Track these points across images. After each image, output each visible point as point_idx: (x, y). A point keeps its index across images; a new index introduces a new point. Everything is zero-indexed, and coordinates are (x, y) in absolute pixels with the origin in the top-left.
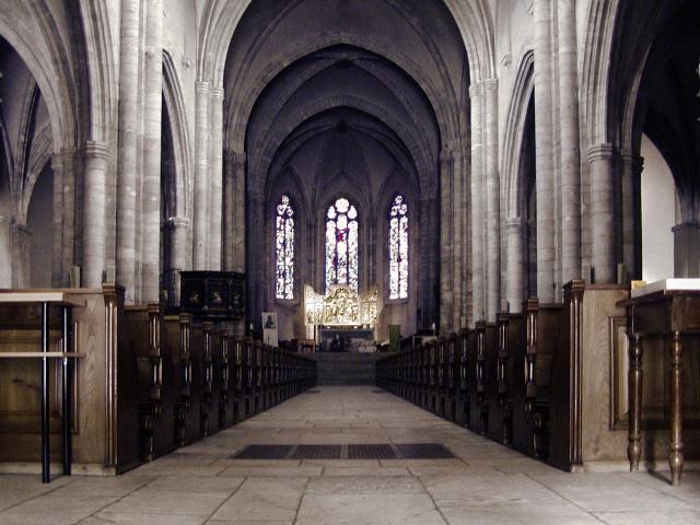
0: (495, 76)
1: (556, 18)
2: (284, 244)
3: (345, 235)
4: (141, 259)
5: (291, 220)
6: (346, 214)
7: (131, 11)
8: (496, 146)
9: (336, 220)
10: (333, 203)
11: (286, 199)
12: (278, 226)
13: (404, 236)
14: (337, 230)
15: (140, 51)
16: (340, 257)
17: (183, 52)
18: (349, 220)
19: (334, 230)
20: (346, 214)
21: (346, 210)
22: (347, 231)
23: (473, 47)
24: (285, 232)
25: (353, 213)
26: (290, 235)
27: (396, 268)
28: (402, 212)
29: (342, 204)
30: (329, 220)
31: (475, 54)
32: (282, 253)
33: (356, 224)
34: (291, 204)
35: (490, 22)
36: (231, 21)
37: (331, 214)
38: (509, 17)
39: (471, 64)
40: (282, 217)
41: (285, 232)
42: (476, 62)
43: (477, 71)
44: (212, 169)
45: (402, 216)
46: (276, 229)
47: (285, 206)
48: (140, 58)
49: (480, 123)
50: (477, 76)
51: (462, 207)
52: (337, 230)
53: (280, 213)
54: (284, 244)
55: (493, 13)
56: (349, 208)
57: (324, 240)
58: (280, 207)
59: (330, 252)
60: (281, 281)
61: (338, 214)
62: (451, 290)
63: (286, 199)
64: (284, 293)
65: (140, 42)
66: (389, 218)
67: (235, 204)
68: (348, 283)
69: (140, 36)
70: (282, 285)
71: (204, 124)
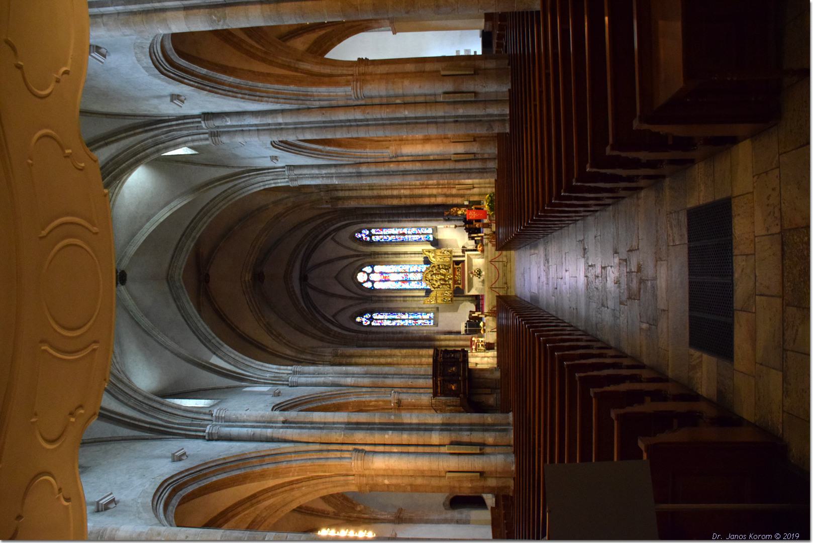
0: (284, 167)
1: (256, 125)
2: (393, 320)
3: (384, 275)
4: (438, 427)
5: (374, 314)
6: (368, 274)
7: (254, 434)
8: (335, 166)
9: (373, 282)
10: (361, 284)
11: (358, 319)
12: (379, 324)
13: (385, 232)
14: (380, 281)
15: (282, 428)
17: (268, 396)
18: (373, 272)
20: (368, 274)
21: (366, 275)
22: (381, 273)
23: (261, 184)
24: (383, 320)
25: (368, 269)
26: (385, 316)
27: (410, 236)
28: (367, 232)
29: (361, 277)
30: (373, 286)
31: (266, 183)
32: (398, 321)
34: (362, 315)
35: (243, 172)
36: (243, 361)
37: (368, 285)
38: (245, 158)
39: (273, 185)
40: (371, 321)
41: (383, 320)
42: (272, 182)
43: (279, 181)
44: (354, 374)
45: (370, 233)
46: (381, 326)
47: (364, 320)
48: (287, 428)
49: (318, 178)
50: (283, 180)
51: (373, 189)
52: (380, 281)
53: (369, 323)
54: (393, 320)
55: (237, 170)
56: (365, 272)
57: (389, 290)
58: (364, 323)
59: (398, 286)
60: (419, 322)
61: (368, 280)
62: (435, 196)
63: (358, 319)
64: (429, 320)
65: (275, 427)
66: (371, 243)
67: (371, 356)
69: (271, 427)
71: (321, 380)
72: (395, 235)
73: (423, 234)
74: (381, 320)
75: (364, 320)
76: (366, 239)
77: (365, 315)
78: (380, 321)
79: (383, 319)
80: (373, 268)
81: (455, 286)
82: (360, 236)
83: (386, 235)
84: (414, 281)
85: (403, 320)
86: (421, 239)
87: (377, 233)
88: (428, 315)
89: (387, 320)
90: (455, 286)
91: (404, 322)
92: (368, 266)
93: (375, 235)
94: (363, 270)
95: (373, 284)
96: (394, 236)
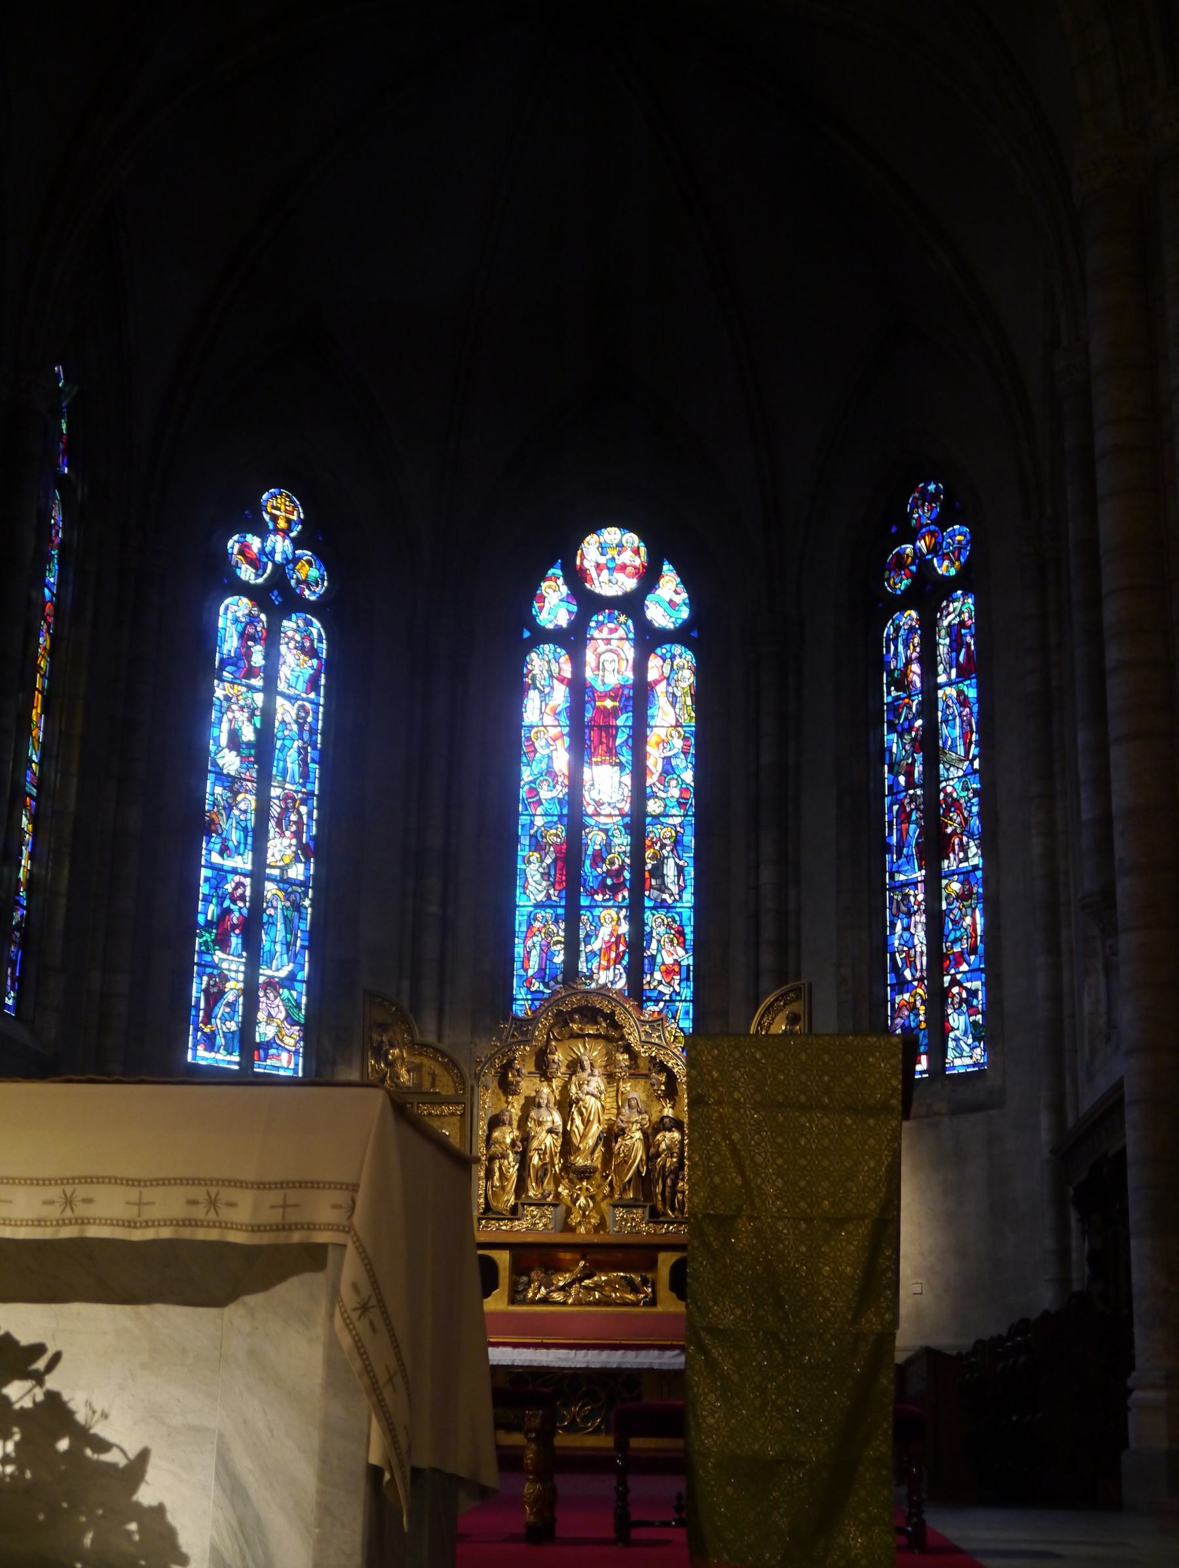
3: (624, 720)
5: (316, 628)
6: (631, 605)
12: (230, 644)
14: (578, 688)
16: (594, 840)
19: (560, 695)
20: (631, 605)
21: (630, 584)
28: (945, 569)
30: (543, 636)
32: (248, 801)
33: (685, 658)
45: (946, 588)
56: (649, 579)
58: (255, 542)
68: (637, 992)
70: (234, 988)
72: (932, 779)
73: (938, 999)
74: (271, 674)
75: (281, 546)
76: (900, 563)
77: (323, 556)
78: (258, 659)
79: (270, 688)
80: (678, 636)
81: (503, 1258)
82: (923, 514)
83: (929, 706)
84: (572, 946)
85: (258, 839)
86: (902, 985)
87: (944, 642)
88: (292, 1038)
89: (268, 714)
90: (503, 1258)
91: (235, 836)
92: (693, 604)
93: (928, 628)
94: (667, 567)
95: (557, 637)
96: (918, 769)
